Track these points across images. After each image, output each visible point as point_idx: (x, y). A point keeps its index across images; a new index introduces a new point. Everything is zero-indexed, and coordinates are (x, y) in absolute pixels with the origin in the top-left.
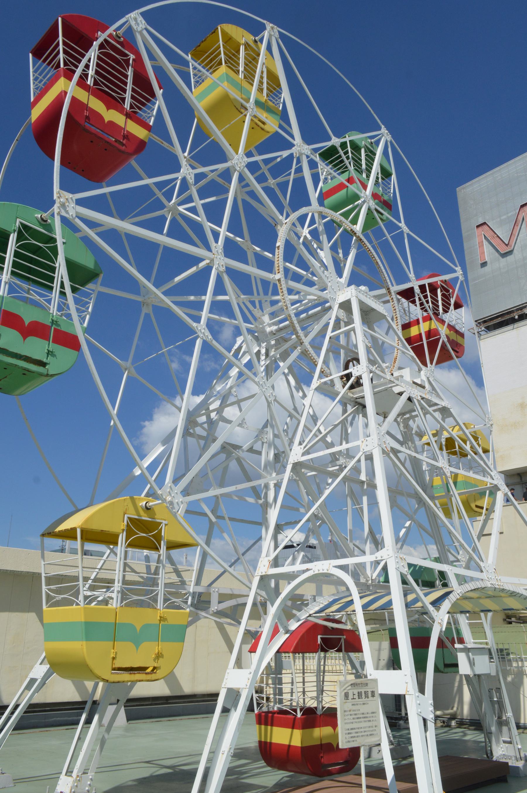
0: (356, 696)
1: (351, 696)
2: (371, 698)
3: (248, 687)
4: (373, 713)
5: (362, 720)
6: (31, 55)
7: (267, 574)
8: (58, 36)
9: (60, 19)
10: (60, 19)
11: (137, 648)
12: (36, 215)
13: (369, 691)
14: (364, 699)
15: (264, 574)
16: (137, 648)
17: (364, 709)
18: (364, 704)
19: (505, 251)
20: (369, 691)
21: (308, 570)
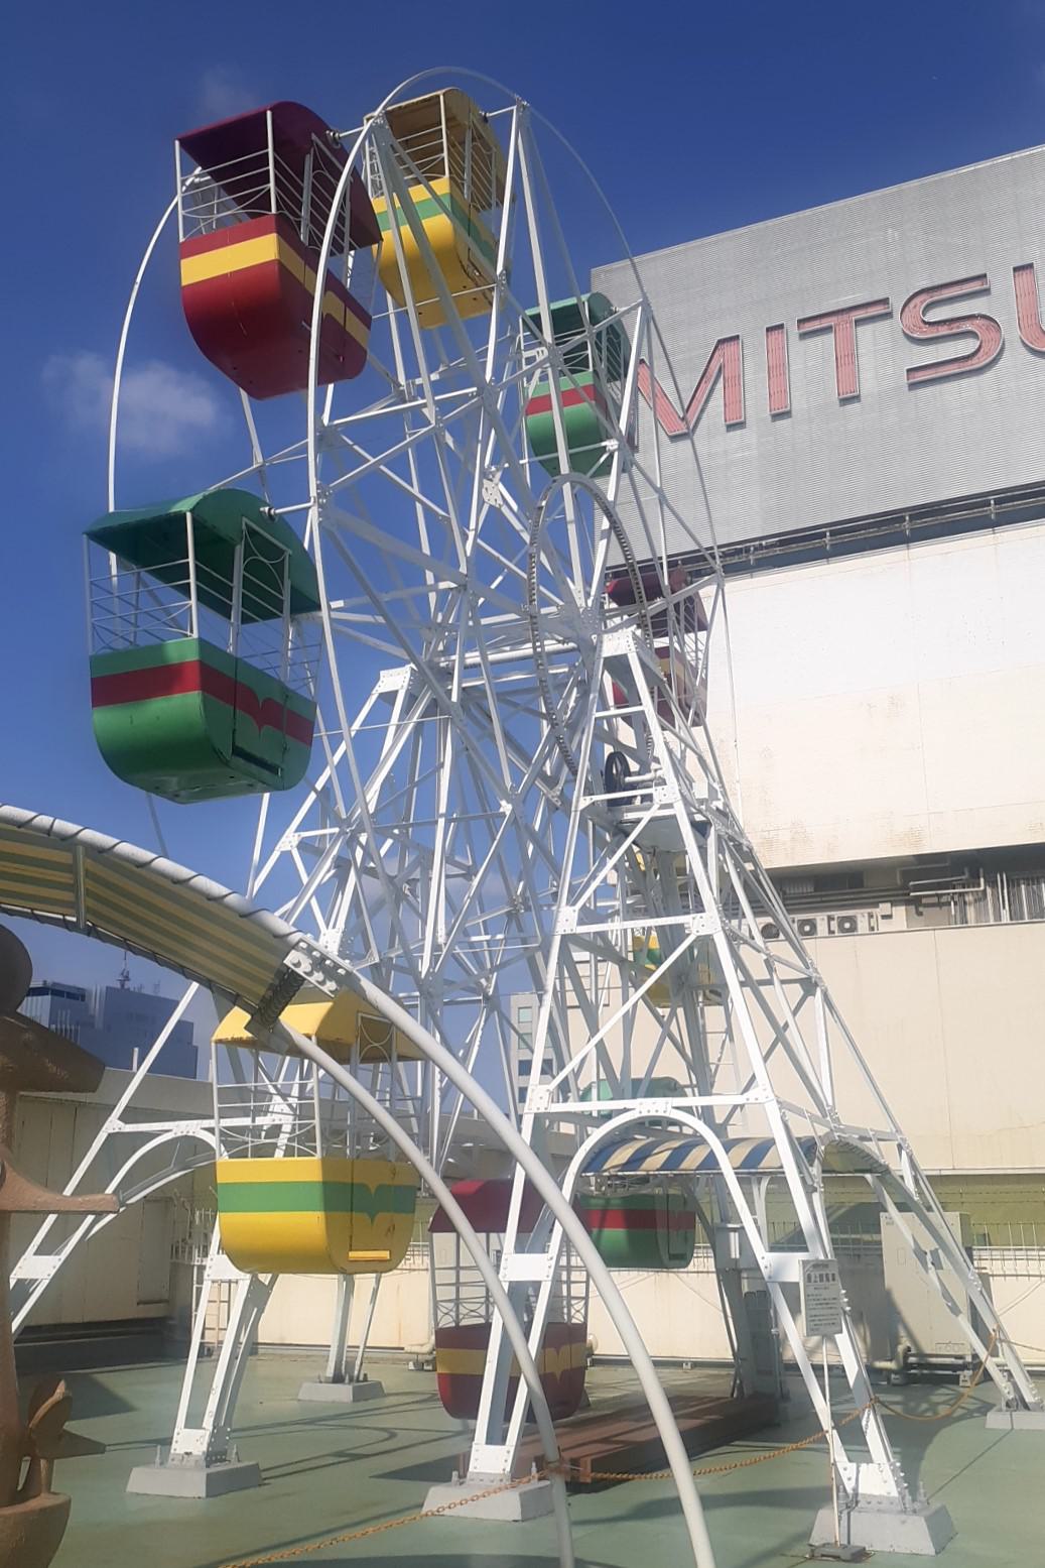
0: (818, 1279)
1: (813, 1279)
2: (831, 1282)
3: (550, 1278)
4: (834, 1299)
5: (824, 1306)
6: (177, 143)
7: (548, 1111)
8: (267, 147)
9: (269, 113)
10: (269, 113)
11: (372, 1221)
12: (262, 509)
13: (830, 1273)
14: (825, 1283)
15: (542, 1110)
16: (372, 1221)
17: (825, 1294)
18: (825, 1288)
19: (677, 433)
20: (830, 1273)
21: (626, 1110)
